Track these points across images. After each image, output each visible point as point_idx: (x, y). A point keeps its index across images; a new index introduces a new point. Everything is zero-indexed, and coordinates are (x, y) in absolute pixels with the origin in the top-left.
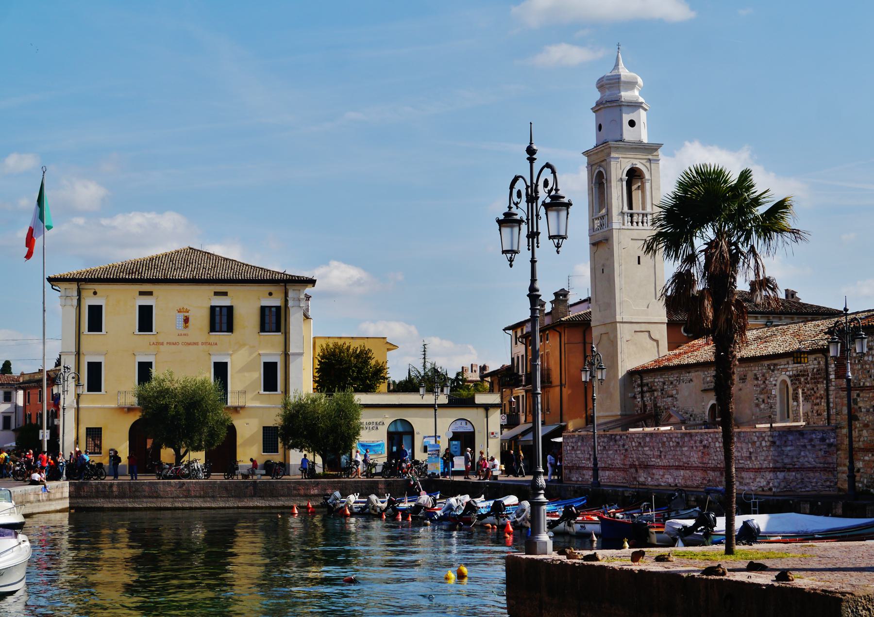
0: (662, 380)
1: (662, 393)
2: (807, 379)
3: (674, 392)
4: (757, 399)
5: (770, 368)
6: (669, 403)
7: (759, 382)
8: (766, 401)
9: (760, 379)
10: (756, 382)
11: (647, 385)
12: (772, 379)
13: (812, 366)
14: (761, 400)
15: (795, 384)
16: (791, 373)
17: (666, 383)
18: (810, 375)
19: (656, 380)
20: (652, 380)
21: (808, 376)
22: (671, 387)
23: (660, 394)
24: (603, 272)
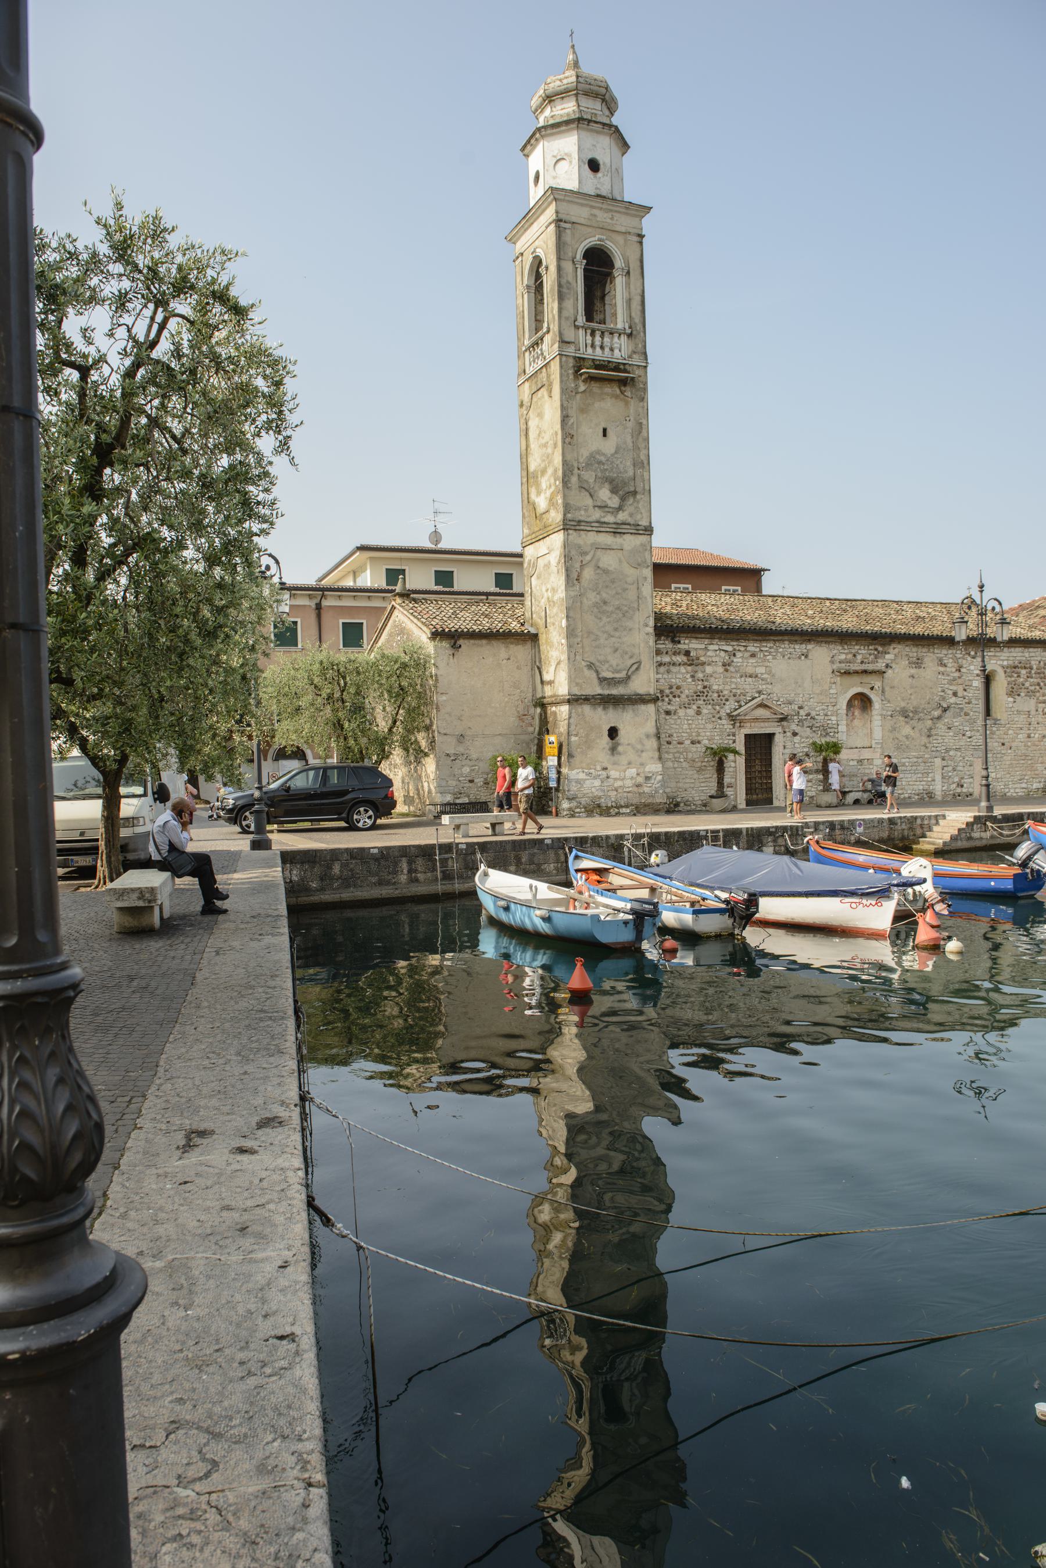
0: (729, 648)
1: (727, 670)
2: (1030, 673)
3: (761, 670)
4: (943, 691)
5: (969, 654)
6: (747, 687)
7: (948, 669)
8: (960, 694)
9: (950, 665)
10: (942, 669)
11: (687, 653)
12: (972, 667)
13: (1039, 658)
14: (951, 692)
15: (1011, 677)
16: (1005, 663)
17: (739, 655)
18: (1035, 667)
19: (711, 647)
20: (703, 646)
21: (1031, 668)
22: (752, 660)
23: (721, 669)
24: (605, 435)
